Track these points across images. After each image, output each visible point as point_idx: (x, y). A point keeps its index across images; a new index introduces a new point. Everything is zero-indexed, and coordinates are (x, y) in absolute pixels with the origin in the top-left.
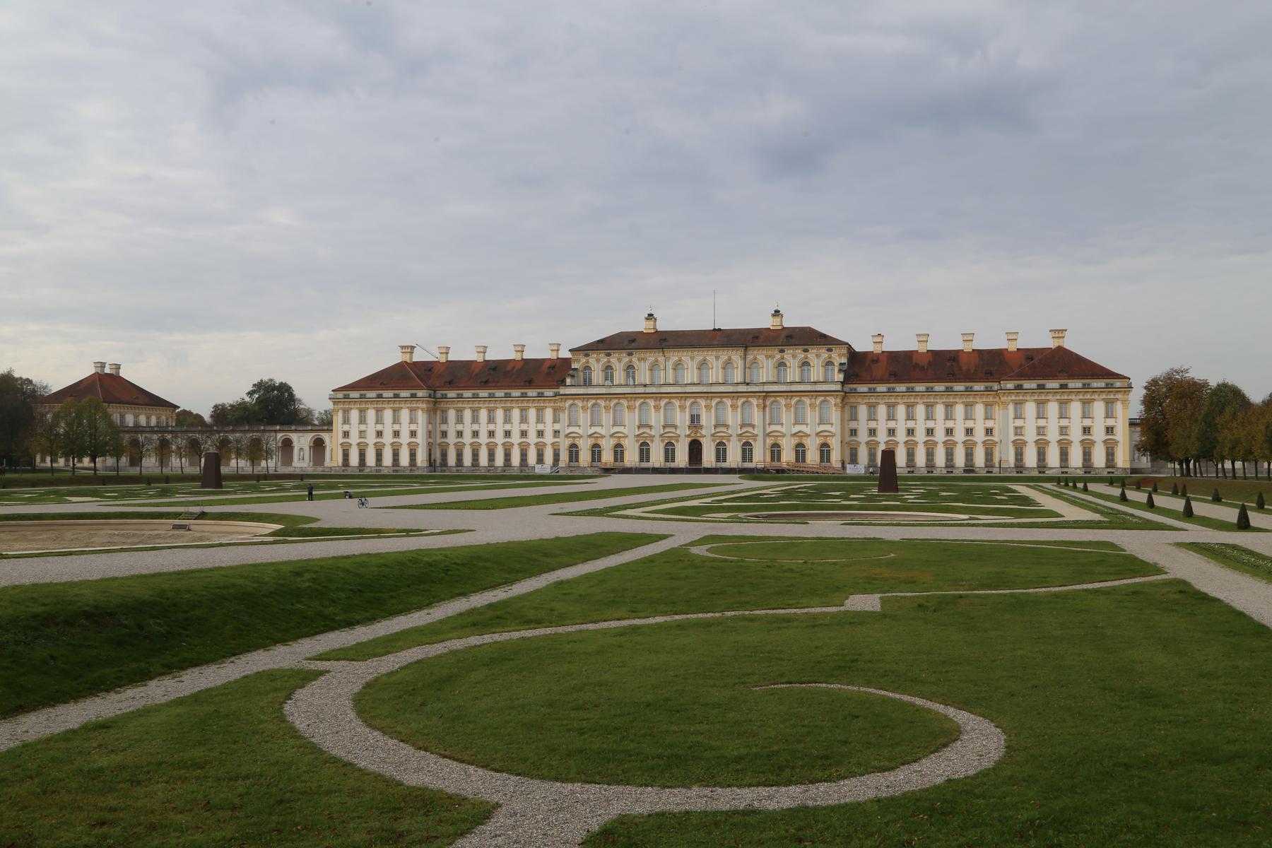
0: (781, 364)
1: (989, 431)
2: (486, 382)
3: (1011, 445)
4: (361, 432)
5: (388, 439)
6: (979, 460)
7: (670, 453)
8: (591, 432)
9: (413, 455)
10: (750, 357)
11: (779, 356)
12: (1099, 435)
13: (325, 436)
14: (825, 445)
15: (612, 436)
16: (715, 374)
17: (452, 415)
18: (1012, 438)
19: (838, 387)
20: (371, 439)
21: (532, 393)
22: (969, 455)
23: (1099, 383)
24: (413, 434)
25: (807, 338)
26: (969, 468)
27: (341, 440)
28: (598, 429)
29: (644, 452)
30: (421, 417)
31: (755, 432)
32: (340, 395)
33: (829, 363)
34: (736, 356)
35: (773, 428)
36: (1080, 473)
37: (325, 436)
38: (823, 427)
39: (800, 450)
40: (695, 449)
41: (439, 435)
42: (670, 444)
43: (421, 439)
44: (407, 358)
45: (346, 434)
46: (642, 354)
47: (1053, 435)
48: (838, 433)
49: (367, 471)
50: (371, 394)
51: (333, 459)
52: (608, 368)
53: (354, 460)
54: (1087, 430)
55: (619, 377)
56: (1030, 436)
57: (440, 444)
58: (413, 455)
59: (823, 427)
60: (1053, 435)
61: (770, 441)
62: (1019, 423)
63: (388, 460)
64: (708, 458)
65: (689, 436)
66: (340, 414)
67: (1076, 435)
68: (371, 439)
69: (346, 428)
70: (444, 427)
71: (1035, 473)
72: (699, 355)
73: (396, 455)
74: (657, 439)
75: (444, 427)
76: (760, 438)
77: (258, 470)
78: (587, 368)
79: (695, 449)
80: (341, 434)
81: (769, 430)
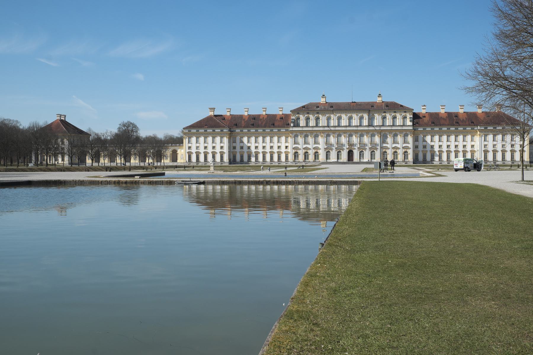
1: (472, 146)
2: (253, 125)
5: (210, 150)
10: (371, 114)
14: (406, 152)
17: (238, 138)
18: (483, 149)
20: (202, 150)
21: (275, 130)
24: (222, 147)
25: (393, 107)
27: (188, 151)
30: (226, 140)
35: (384, 145)
40: (350, 154)
41: (232, 148)
43: (226, 150)
44: (211, 113)
45: (190, 148)
48: (412, 148)
49: (200, 164)
50: (202, 131)
51: (182, 159)
52: (308, 119)
53: (194, 159)
55: (312, 123)
56: (490, 148)
57: (233, 152)
62: (486, 143)
64: (356, 158)
66: (187, 140)
68: (202, 150)
69: (190, 145)
70: (234, 145)
71: (492, 163)
75: (234, 145)
76: (379, 150)
77: (113, 164)
78: (298, 118)
79: (350, 154)
80: (187, 148)
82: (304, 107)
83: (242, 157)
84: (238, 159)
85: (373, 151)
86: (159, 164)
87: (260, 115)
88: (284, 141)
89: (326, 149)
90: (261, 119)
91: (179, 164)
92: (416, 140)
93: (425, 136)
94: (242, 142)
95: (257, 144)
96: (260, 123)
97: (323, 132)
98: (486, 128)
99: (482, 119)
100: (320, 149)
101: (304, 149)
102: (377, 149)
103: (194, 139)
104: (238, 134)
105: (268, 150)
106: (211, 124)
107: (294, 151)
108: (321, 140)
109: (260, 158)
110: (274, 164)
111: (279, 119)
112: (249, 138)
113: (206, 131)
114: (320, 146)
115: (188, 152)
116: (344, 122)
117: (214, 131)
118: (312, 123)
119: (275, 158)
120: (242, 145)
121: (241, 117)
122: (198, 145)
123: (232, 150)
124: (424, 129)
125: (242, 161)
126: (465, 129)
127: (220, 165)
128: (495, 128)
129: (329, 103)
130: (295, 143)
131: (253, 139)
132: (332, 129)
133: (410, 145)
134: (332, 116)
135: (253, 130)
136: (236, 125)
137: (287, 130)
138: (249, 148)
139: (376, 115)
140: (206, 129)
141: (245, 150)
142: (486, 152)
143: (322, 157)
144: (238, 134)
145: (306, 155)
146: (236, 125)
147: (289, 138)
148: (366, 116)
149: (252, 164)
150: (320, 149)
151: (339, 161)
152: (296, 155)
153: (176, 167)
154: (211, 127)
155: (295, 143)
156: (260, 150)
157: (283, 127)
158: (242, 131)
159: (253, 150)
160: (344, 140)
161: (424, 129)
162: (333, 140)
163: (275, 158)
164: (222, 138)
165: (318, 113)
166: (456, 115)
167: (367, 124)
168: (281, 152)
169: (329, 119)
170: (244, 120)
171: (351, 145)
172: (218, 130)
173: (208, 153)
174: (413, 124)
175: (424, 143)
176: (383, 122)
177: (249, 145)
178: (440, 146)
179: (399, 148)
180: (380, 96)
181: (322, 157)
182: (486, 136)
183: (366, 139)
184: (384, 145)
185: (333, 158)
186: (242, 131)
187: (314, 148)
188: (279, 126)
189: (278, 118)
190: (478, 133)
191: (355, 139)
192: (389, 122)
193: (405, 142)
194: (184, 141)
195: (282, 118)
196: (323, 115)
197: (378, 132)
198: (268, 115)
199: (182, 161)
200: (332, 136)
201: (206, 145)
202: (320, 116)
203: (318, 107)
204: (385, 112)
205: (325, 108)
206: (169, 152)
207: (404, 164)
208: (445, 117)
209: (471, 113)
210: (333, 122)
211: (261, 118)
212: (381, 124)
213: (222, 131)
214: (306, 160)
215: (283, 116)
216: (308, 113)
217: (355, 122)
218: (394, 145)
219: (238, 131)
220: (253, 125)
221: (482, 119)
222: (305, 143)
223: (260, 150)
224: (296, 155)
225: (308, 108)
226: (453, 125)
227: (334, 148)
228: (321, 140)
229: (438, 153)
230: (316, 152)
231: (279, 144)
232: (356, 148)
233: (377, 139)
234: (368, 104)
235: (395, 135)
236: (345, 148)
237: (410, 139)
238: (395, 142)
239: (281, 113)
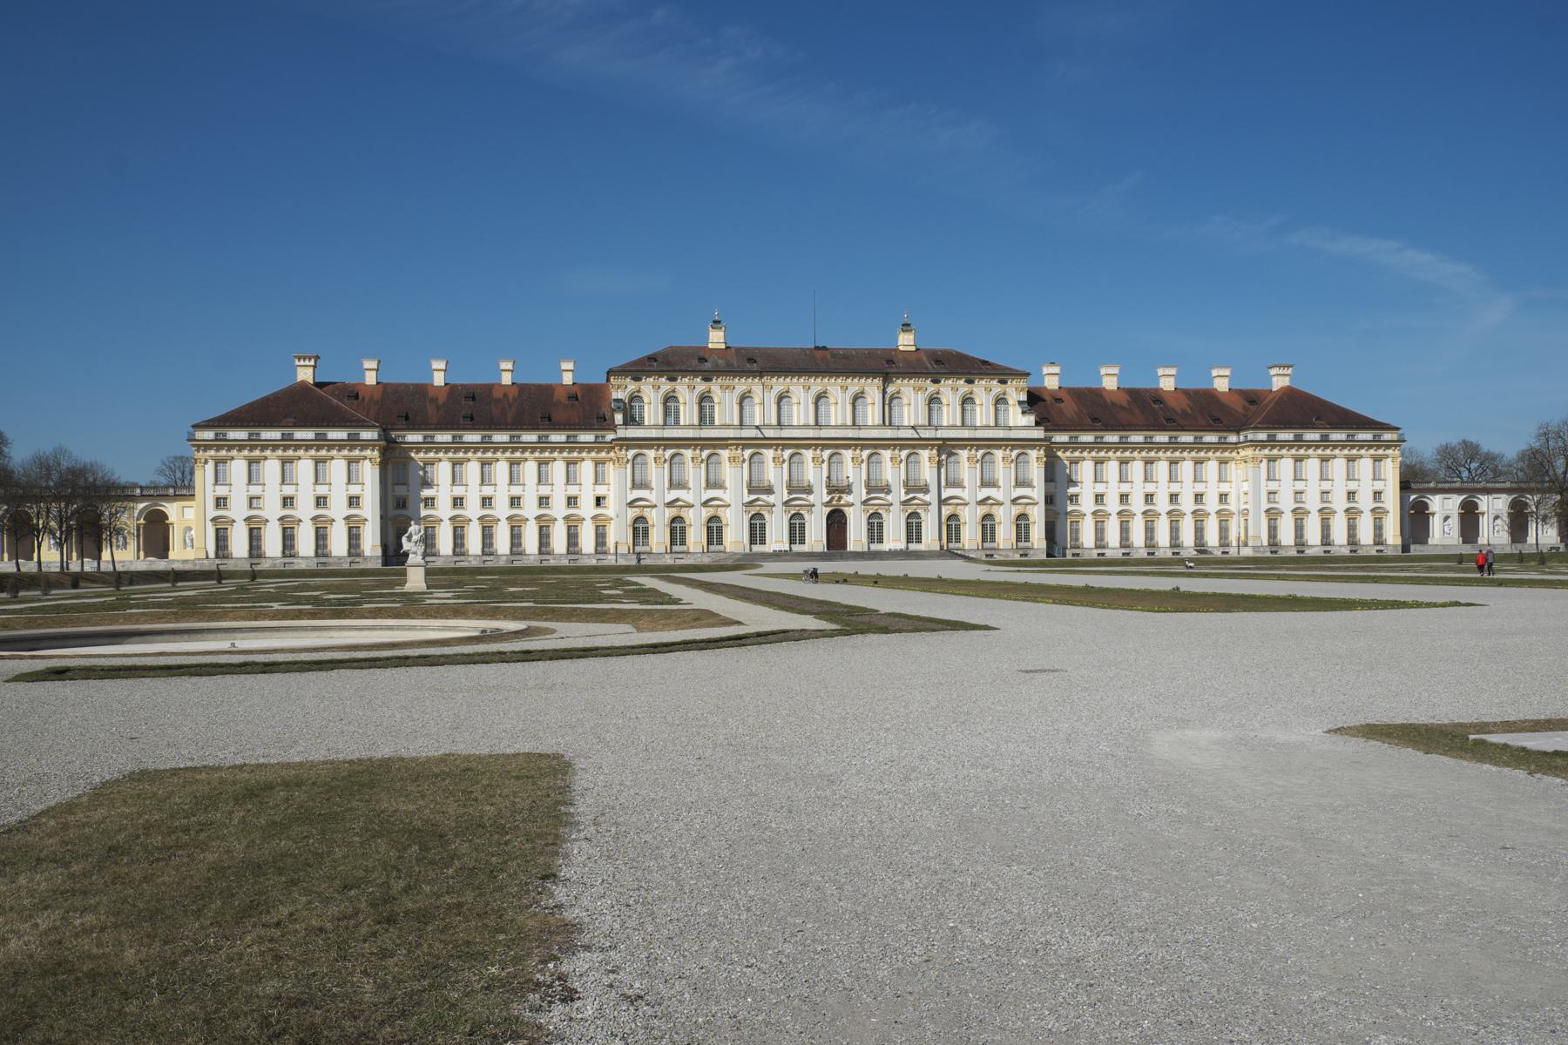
0: (933, 400)
1: (1223, 497)
3: (1263, 515)
4: (251, 499)
5: (305, 509)
6: (1212, 538)
7: (796, 532)
9: (354, 538)
10: (891, 389)
11: (932, 388)
12: (1365, 502)
13: (172, 510)
15: (705, 504)
16: (837, 413)
18: (1265, 506)
19: (1039, 433)
20: (272, 510)
21: (558, 437)
22: (1199, 532)
23: (1366, 436)
24: (353, 501)
27: (212, 512)
29: (757, 532)
30: (369, 472)
31: (927, 498)
32: (209, 435)
33: (1000, 401)
34: (872, 388)
36: (1346, 551)
37: (172, 510)
39: (988, 526)
40: (836, 522)
41: (391, 504)
42: (797, 515)
43: (370, 509)
44: (305, 374)
45: (221, 502)
46: (728, 381)
47: (1313, 503)
49: (265, 565)
52: (669, 399)
53: (239, 546)
54: (1351, 495)
55: (688, 413)
56: (1286, 503)
58: (354, 538)
60: (1313, 503)
61: (946, 511)
62: (1273, 486)
63: (305, 544)
64: (856, 536)
65: (828, 504)
66: (210, 466)
67: (1339, 503)
68: (272, 510)
69: (222, 491)
70: (401, 491)
72: (817, 384)
73: (321, 537)
74: (779, 508)
75: (401, 491)
79: (836, 522)
80: (211, 503)
81: (944, 496)
82: (652, 358)
86: (90, 565)
88: (592, 480)
90: (498, 401)
91: (178, 567)
92: (1050, 477)
97: (744, 443)
99: (1240, 410)
103: (238, 468)
107: (632, 513)
110: (553, 562)
111: (564, 400)
115: (214, 520)
116: (800, 412)
118: (688, 413)
122: (255, 490)
123: (392, 512)
127: (346, 566)
129: (738, 350)
132: (769, 433)
133: (1037, 492)
136: (407, 418)
140: (287, 431)
142: (1273, 515)
145: (677, 530)
146: (407, 418)
147: (610, 467)
152: (640, 529)
157: (587, 427)
160: (812, 470)
162: (773, 471)
166: (1157, 397)
167: (878, 421)
170: (434, 400)
171: (836, 489)
174: (1037, 424)
180: (906, 327)
183: (890, 469)
189: (560, 396)
192: (949, 414)
194: (198, 474)
198: (523, 389)
199: (190, 554)
203: (703, 360)
205: (729, 364)
206: (131, 517)
207: (1017, 557)
208: (1125, 404)
209: (1197, 392)
211: (497, 394)
214: (676, 548)
215: (576, 388)
220: (472, 419)
221: (1240, 410)
222: (673, 485)
224: (640, 529)
225: (668, 364)
231: (573, 490)
233: (926, 469)
234: (871, 354)
237: (1035, 470)
239: (568, 379)
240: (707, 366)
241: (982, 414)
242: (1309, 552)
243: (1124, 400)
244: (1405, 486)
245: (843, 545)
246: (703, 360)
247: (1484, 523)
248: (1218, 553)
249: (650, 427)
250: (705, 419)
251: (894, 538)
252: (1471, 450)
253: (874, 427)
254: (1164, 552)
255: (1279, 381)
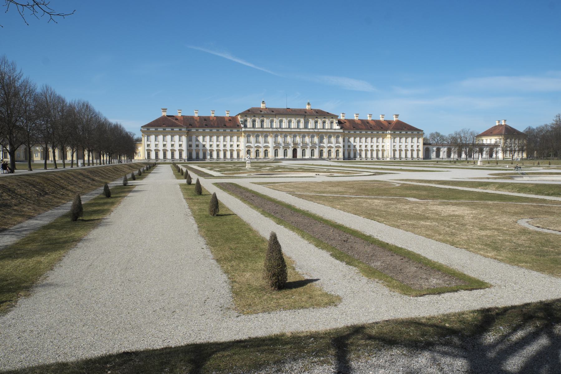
1: (383, 146)
5: (169, 148)
8: (256, 145)
12: (415, 148)
17: (194, 137)
18: (393, 148)
19: (341, 131)
20: (161, 148)
23: (415, 133)
24: (180, 145)
26: (378, 158)
27: (146, 148)
28: (259, 144)
30: (184, 138)
35: (322, 145)
38: (337, 145)
40: (295, 151)
43: (184, 147)
44: (165, 114)
45: (148, 145)
50: (160, 129)
53: (153, 156)
55: (258, 125)
56: (397, 148)
59: (337, 145)
60: (403, 148)
62: (395, 144)
64: (299, 155)
66: (146, 138)
67: (409, 148)
68: (161, 148)
69: (149, 143)
70: (190, 143)
75: (190, 143)
78: (246, 121)
79: (295, 151)
80: (146, 146)
82: (249, 111)
83: (197, 154)
84: (194, 156)
85: (304, 150)
87: (209, 117)
88: (236, 140)
89: (274, 147)
93: (349, 138)
94: (197, 140)
95: (210, 142)
96: (212, 123)
97: (273, 132)
98: (394, 132)
100: (269, 147)
101: (256, 147)
102: (316, 148)
104: (194, 133)
105: (221, 148)
106: (165, 124)
107: (247, 149)
108: (270, 139)
109: (215, 155)
110: (227, 161)
112: (204, 137)
113: (164, 130)
114: (270, 145)
115: (147, 150)
116: (285, 125)
117: (172, 130)
118: (258, 125)
119: (228, 156)
120: (197, 143)
121: (192, 118)
122: (157, 143)
124: (349, 132)
125: (197, 158)
126: (378, 133)
128: (400, 132)
129: (269, 109)
130: (248, 142)
131: (208, 138)
133: (341, 145)
134: (275, 119)
135: (208, 130)
137: (238, 131)
138: (204, 146)
139: (310, 120)
141: (201, 147)
142: (395, 151)
143: (271, 154)
144: (194, 133)
145: (257, 152)
148: (302, 120)
149: (207, 161)
150: (269, 147)
151: (286, 157)
153: (450, 162)
154: (169, 126)
155: (248, 142)
156: (215, 148)
158: (197, 130)
159: (208, 147)
160: (289, 139)
161: (349, 132)
162: (280, 139)
163: (228, 156)
164: (180, 136)
165: (263, 116)
167: (303, 127)
168: (213, 150)
169: (272, 122)
170: (196, 120)
171: (295, 144)
172: (176, 129)
173: (159, 150)
175: (349, 144)
176: (316, 126)
177: (204, 143)
178: (360, 146)
179: (332, 147)
180: (309, 104)
181: (271, 154)
182: (394, 138)
183: (307, 140)
184: (322, 145)
185: (281, 155)
186: (197, 130)
187: (264, 147)
188: (230, 127)
189: (227, 119)
190: (389, 136)
191: (298, 139)
192: (320, 126)
193: (337, 142)
195: (230, 120)
196: (267, 118)
197: (317, 134)
198: (217, 117)
200: (260, 137)
201: (165, 143)
202: (265, 119)
204: (317, 118)
210: (276, 125)
211: (211, 119)
212: (314, 127)
213: (180, 130)
216: (254, 116)
217: (294, 125)
218: (329, 145)
219: (194, 130)
222: (257, 142)
223: (215, 148)
226: (369, 130)
227: (281, 147)
228: (270, 139)
229: (359, 152)
230: (266, 150)
232: (300, 147)
233: (316, 140)
234: (300, 110)
235: (330, 137)
236: (290, 146)
237: (341, 140)
238: (329, 142)
240: (262, 113)
241: (327, 126)
242: (402, 160)
243: (360, 122)
244: (424, 144)
245: (296, 157)
246: (261, 111)
247: (441, 153)
248: (381, 160)
249: (249, 128)
250: (262, 126)
251: (308, 156)
252: (438, 134)
253: (302, 129)
254: (369, 160)
255: (395, 119)
